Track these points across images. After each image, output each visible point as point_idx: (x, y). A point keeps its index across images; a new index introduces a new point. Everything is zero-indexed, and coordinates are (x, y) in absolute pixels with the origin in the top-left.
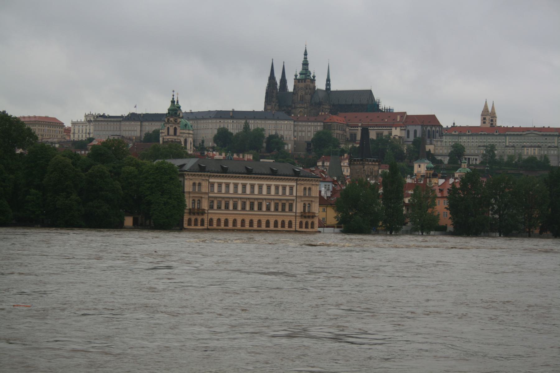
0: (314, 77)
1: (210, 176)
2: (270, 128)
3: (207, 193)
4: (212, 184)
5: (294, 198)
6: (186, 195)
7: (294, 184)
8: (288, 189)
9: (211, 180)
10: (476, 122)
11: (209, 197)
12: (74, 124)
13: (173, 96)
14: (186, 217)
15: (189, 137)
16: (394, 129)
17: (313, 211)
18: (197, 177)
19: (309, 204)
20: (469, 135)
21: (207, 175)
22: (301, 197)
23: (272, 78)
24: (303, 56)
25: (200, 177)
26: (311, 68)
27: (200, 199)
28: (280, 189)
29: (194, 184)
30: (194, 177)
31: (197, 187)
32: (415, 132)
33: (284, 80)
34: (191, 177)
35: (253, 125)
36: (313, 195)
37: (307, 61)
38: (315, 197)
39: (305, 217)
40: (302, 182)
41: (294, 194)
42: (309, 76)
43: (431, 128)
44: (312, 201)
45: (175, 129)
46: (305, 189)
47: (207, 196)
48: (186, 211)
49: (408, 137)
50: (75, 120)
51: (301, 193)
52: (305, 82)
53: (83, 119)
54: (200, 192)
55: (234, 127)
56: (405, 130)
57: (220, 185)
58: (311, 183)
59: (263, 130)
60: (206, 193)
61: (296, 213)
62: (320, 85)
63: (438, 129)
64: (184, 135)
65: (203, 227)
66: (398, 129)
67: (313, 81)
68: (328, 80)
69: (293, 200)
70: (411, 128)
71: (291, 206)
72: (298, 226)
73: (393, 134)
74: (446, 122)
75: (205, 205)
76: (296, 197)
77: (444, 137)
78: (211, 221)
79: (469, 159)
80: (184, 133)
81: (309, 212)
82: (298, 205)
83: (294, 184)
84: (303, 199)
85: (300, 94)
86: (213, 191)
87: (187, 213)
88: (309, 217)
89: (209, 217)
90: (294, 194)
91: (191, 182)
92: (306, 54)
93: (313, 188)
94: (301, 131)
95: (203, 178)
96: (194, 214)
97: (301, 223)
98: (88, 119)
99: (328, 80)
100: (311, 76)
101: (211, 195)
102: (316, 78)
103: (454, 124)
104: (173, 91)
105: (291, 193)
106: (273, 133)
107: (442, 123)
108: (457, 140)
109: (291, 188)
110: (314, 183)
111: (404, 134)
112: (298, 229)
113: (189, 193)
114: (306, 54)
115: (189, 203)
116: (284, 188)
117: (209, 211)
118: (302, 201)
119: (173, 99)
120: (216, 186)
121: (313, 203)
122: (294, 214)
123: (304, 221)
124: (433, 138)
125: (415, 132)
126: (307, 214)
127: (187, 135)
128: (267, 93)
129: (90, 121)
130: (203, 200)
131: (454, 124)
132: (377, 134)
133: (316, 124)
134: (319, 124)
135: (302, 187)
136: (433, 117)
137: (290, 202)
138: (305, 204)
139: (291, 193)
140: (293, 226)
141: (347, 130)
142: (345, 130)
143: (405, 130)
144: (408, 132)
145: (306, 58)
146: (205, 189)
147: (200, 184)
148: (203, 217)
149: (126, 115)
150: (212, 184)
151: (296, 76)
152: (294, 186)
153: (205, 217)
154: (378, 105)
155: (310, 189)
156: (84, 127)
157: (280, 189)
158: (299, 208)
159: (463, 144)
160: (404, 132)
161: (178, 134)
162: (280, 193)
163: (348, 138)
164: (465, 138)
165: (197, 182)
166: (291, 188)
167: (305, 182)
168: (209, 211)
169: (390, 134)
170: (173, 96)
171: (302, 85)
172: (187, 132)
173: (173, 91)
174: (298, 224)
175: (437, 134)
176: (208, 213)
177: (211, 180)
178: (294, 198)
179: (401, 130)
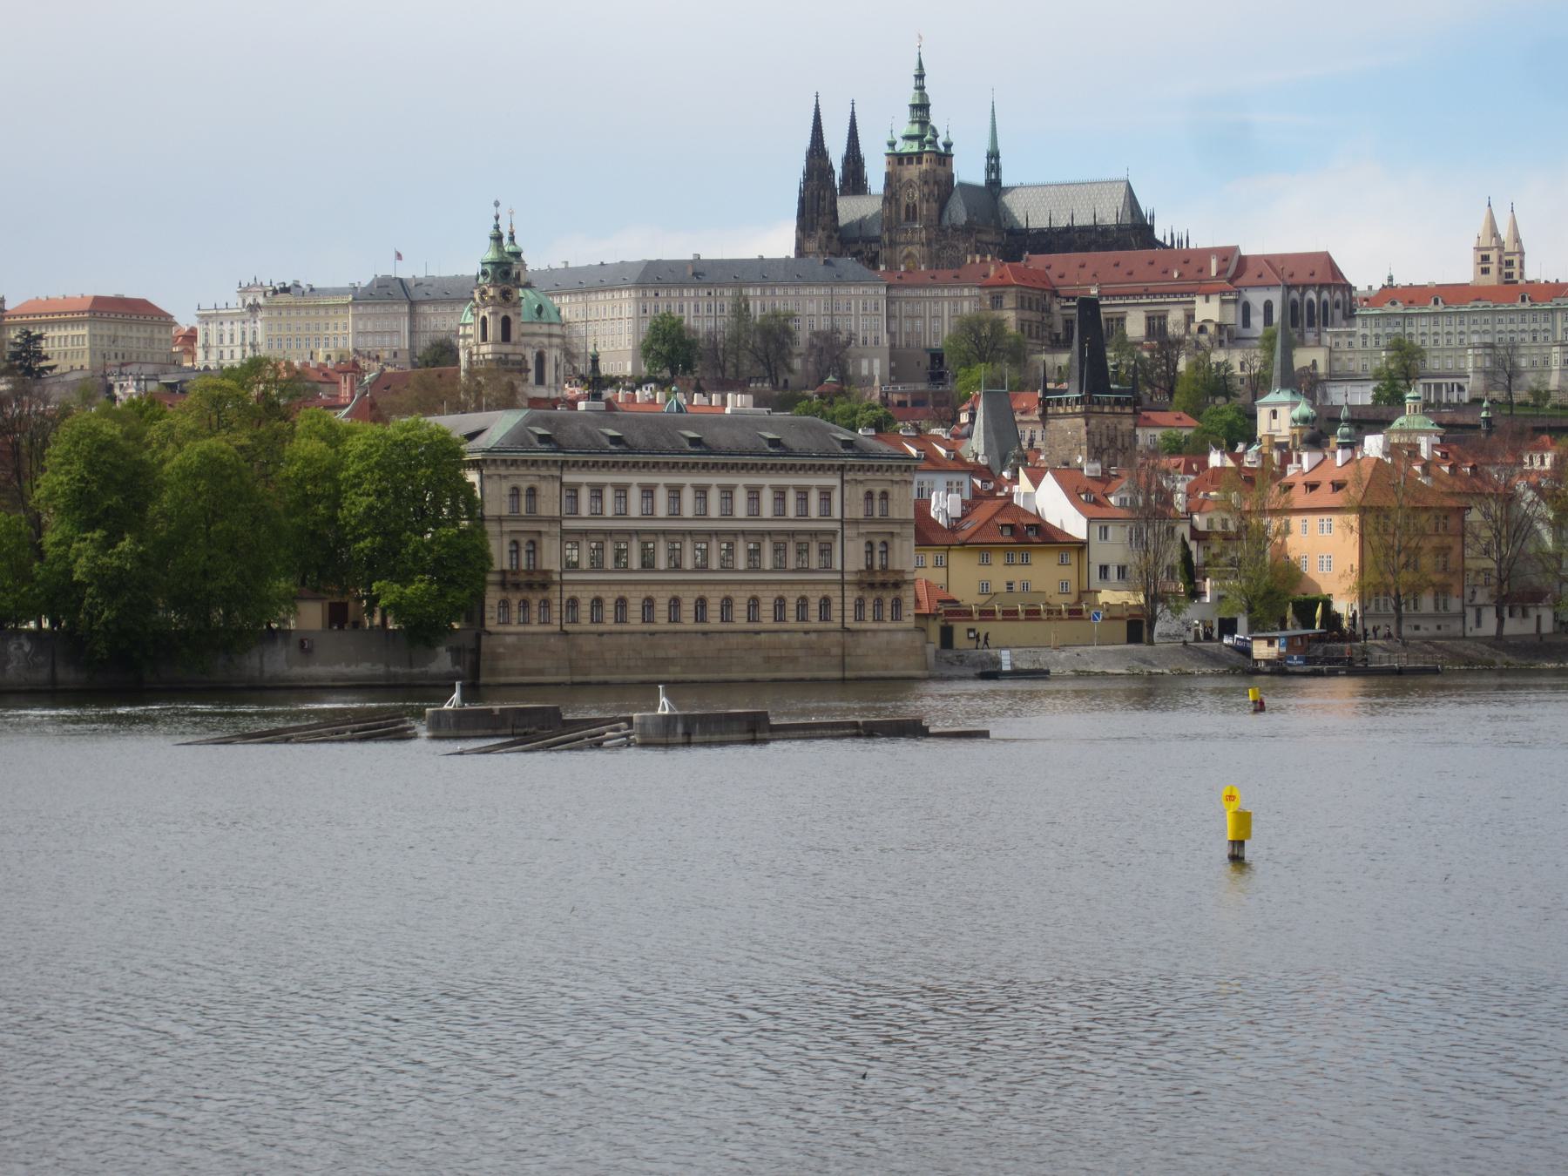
0: (948, 145)
1: (564, 465)
2: (811, 310)
3: (556, 520)
4: (574, 490)
5: (837, 526)
6: (491, 528)
8: (814, 498)
9: (569, 478)
10: (1463, 271)
11: (564, 532)
12: (205, 318)
13: (497, 218)
14: (493, 597)
15: (551, 346)
16: (1199, 300)
17: (897, 567)
18: (523, 470)
19: (885, 543)
20: (1436, 314)
21: (555, 462)
22: (856, 522)
23: (817, 150)
24: (912, 82)
25: (533, 470)
26: (935, 120)
27: (534, 538)
28: (791, 497)
29: (515, 492)
30: (513, 470)
31: (523, 500)
32: (1268, 307)
33: (854, 159)
34: (503, 471)
35: (759, 304)
36: (895, 513)
37: (923, 95)
38: (903, 522)
39: (872, 586)
40: (860, 476)
41: (837, 514)
42: (933, 143)
43: (1319, 295)
44: (892, 534)
45: (506, 322)
46: (869, 495)
48: (491, 578)
49: (1246, 322)
50: (208, 306)
52: (920, 161)
53: (235, 302)
54: (532, 516)
55: (701, 316)
56: (1236, 301)
57: (597, 491)
58: (888, 476)
59: (790, 316)
60: (552, 520)
61: (842, 572)
62: (968, 170)
63: (1338, 295)
64: (536, 340)
65: (548, 628)
66: (1215, 301)
67: (944, 158)
68: (994, 155)
69: (833, 533)
70: (1256, 298)
71: (826, 551)
72: (850, 613)
73: (1199, 318)
74: (1363, 274)
75: (550, 557)
76: (842, 521)
77: (1359, 321)
78: (573, 603)
79: (1438, 387)
80: (534, 335)
81: (884, 569)
82: (849, 546)
83: (833, 481)
84: (864, 529)
85: (904, 200)
86: (575, 513)
87: (494, 583)
88: (884, 585)
89: (566, 596)
90: (837, 514)
91: (506, 487)
92: (920, 76)
93: (895, 492)
94: (913, 317)
95: (544, 472)
96: (517, 586)
97: (860, 604)
98: (250, 300)
99: (994, 155)
100: (940, 142)
101: (568, 524)
102: (953, 150)
103: (1390, 279)
104: (497, 204)
105: (826, 512)
106: (823, 324)
107: (1351, 277)
108: (1398, 330)
109: (826, 494)
110: (897, 476)
111: (1233, 316)
112: (850, 623)
113: (500, 519)
114: (920, 76)
115: (499, 553)
116: (803, 493)
117: (566, 577)
118: (860, 535)
119: (497, 227)
120: (584, 495)
121: (897, 541)
122: (838, 577)
124: (1326, 324)
125: (1268, 307)
126: (879, 578)
127: (546, 341)
128: (802, 201)
129: (254, 308)
130: (545, 541)
131: (1390, 279)
132: (1149, 319)
133: (957, 292)
134: (966, 292)
135: (861, 491)
136: (1326, 261)
138: (870, 544)
139: (826, 512)
140: (836, 613)
141: (1056, 308)
142: (1047, 310)
143: (1236, 301)
144: (1246, 308)
145: (921, 88)
146: (549, 504)
147: (532, 492)
148: (545, 594)
149: (365, 283)
150: (574, 490)
151: (892, 144)
152: (833, 488)
153: (554, 595)
154: (1151, 229)
155: (885, 495)
156: (237, 326)
157: (791, 497)
158: (853, 556)
159: (1417, 341)
160: (1231, 308)
161: (514, 336)
162: (791, 512)
163: (1058, 335)
164: (1424, 321)
165: (524, 486)
166: (826, 494)
167: (869, 475)
168: (566, 577)
169: (1190, 317)
170: (497, 218)
171: (912, 172)
172: (545, 329)
173: (497, 204)
174: (850, 606)
175: (1338, 313)
176: (562, 583)
177: (569, 478)
178: (837, 526)
179: (1223, 302)
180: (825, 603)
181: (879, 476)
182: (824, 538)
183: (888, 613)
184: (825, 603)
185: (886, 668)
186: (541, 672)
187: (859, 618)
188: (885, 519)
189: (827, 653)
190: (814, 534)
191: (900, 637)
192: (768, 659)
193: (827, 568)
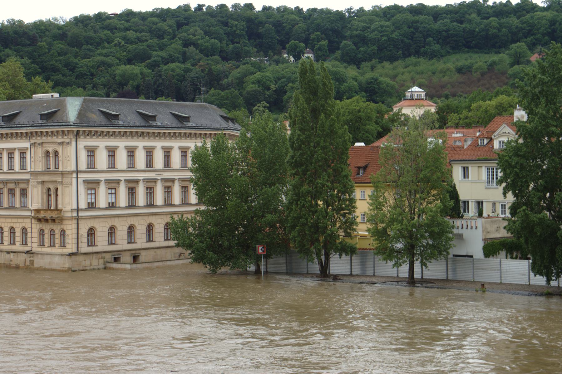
5: (27, 177)
7: (24, 144)
40: (39, 140)
46: (47, 153)
72: (36, 240)
81: (57, 209)
97: (42, 233)
105: (23, 167)
110: (60, 139)
123: (47, 228)
135: (40, 152)
137: (22, 186)
139: (23, 167)
152: (28, 148)
155: (56, 153)
167: (44, 139)
174: (36, 235)
180: (24, 231)
181: (49, 139)
183: (57, 241)
184: (24, 231)
187: (42, 244)
188: (56, 172)
190: (17, 182)
191: (57, 259)
193: (24, 207)
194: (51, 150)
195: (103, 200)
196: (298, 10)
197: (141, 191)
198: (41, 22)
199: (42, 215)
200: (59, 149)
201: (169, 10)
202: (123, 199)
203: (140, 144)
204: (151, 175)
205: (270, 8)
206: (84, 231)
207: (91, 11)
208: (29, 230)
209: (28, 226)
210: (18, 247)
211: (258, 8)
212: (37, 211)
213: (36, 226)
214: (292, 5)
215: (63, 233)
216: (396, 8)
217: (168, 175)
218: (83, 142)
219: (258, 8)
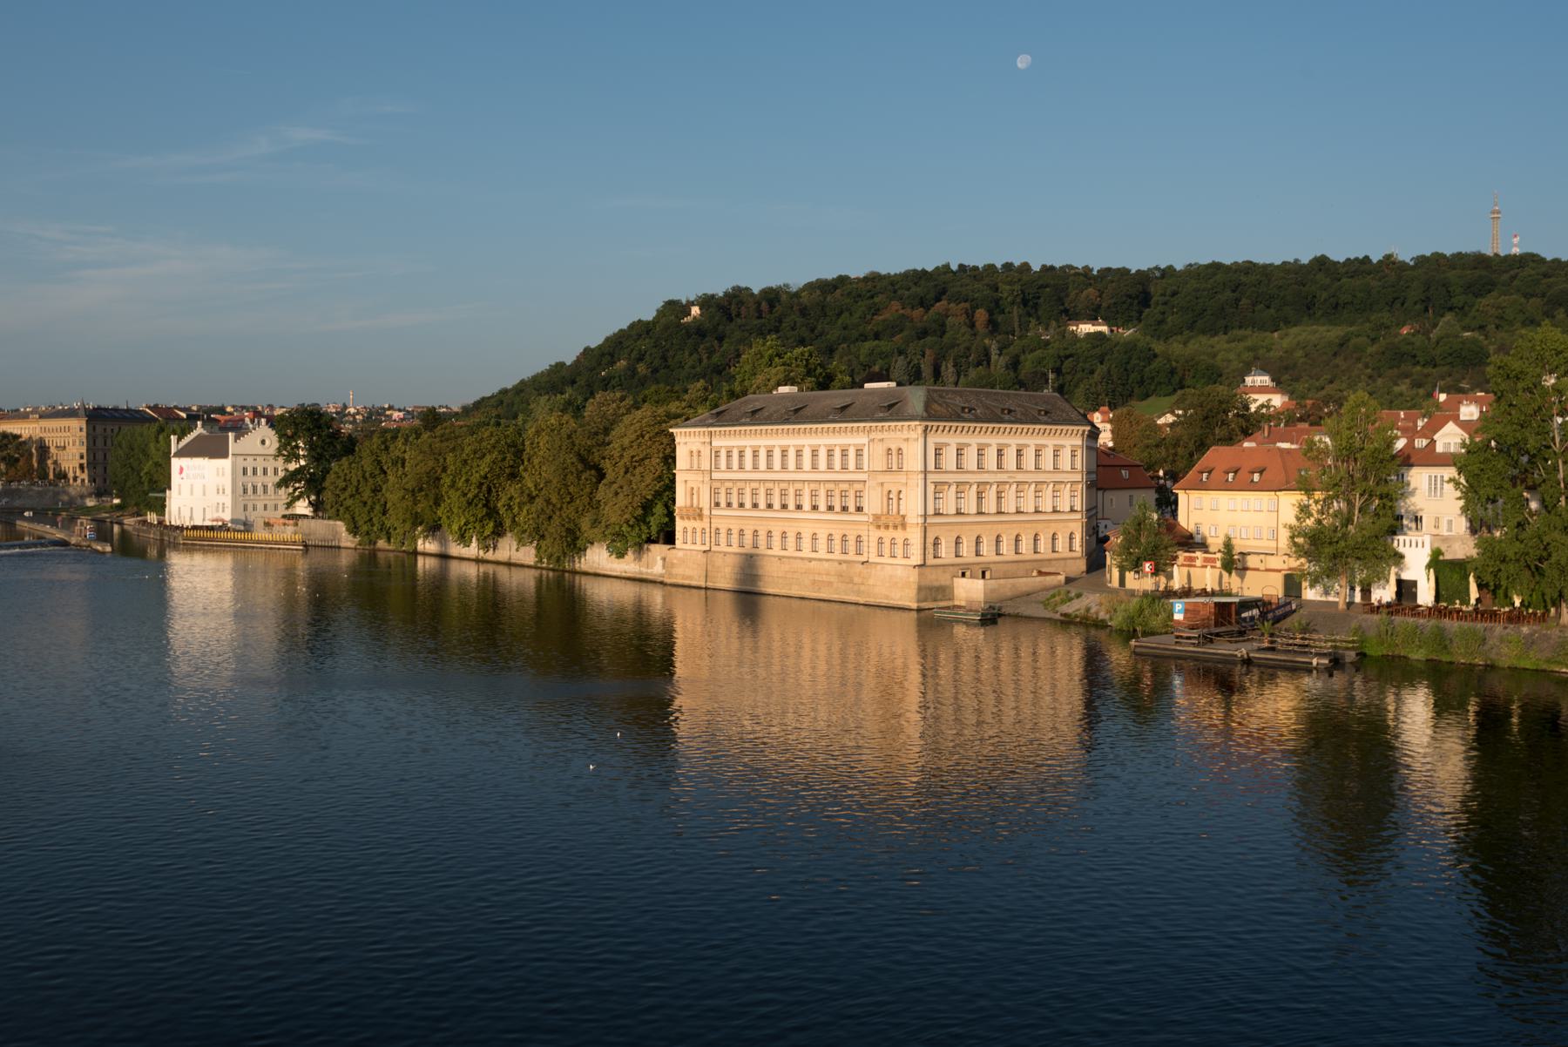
7: (862, 440)
40: (880, 435)
47: (707, 479)
51: (880, 465)
72: (874, 550)
84: (881, 478)
97: (880, 541)
101: (715, 476)
105: (859, 467)
109: (859, 453)
112: (873, 558)
123: (887, 535)
135: (880, 449)
137: (858, 486)
139: (859, 467)
157: (837, 454)
174: (874, 544)
180: (859, 540)
182: (858, 486)
184: (859, 540)
185: (887, 597)
186: (690, 578)
189: (851, 581)
190: (851, 482)
192: (814, 582)
194: (894, 447)
195: (948, 505)
196: (1087, 270)
197: (991, 495)
198: (771, 289)
199: (884, 520)
200: (904, 446)
201: (924, 272)
202: (970, 505)
203: (993, 441)
204: (1002, 477)
205: (1052, 268)
206: (930, 540)
207: (830, 274)
208: (864, 538)
209: (864, 534)
210: (851, 556)
211: (1036, 267)
212: (877, 517)
213: (875, 534)
214: (1079, 264)
215: (906, 543)
216: (1216, 267)
217: (1020, 477)
218: (933, 440)
219: (1036, 267)
